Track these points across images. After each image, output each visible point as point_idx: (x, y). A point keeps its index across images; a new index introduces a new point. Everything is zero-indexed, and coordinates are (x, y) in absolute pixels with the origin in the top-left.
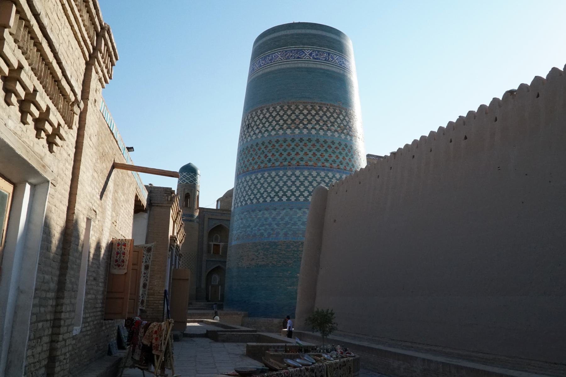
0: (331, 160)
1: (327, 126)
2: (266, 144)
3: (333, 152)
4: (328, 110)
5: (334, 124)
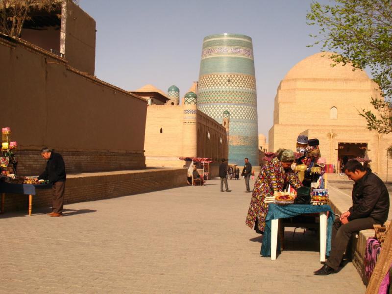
2: (241, 92)
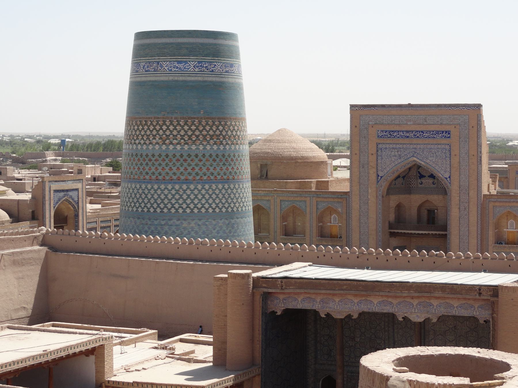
0: (150, 172)
1: (150, 140)
3: (153, 164)
4: (152, 124)
5: (156, 137)
